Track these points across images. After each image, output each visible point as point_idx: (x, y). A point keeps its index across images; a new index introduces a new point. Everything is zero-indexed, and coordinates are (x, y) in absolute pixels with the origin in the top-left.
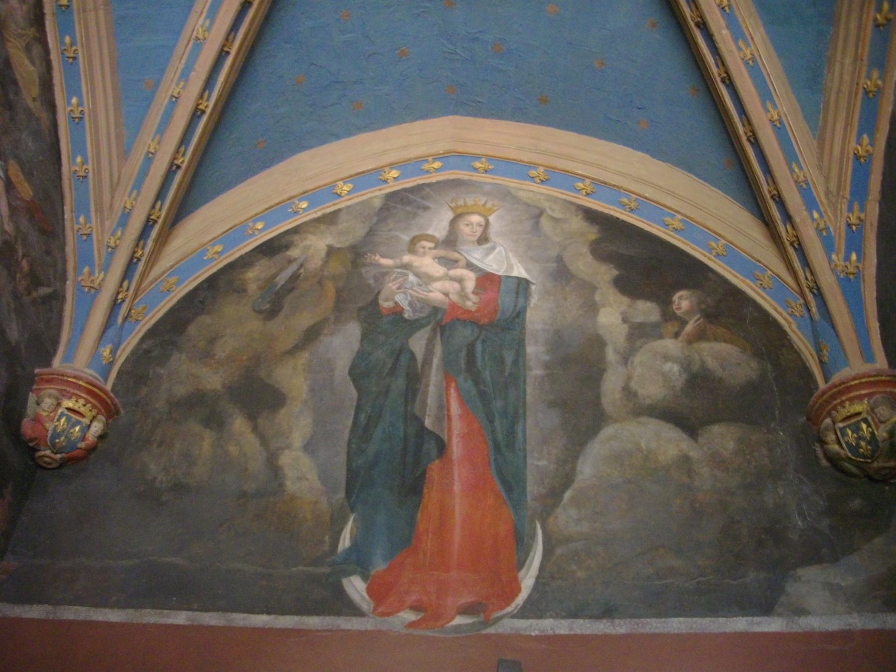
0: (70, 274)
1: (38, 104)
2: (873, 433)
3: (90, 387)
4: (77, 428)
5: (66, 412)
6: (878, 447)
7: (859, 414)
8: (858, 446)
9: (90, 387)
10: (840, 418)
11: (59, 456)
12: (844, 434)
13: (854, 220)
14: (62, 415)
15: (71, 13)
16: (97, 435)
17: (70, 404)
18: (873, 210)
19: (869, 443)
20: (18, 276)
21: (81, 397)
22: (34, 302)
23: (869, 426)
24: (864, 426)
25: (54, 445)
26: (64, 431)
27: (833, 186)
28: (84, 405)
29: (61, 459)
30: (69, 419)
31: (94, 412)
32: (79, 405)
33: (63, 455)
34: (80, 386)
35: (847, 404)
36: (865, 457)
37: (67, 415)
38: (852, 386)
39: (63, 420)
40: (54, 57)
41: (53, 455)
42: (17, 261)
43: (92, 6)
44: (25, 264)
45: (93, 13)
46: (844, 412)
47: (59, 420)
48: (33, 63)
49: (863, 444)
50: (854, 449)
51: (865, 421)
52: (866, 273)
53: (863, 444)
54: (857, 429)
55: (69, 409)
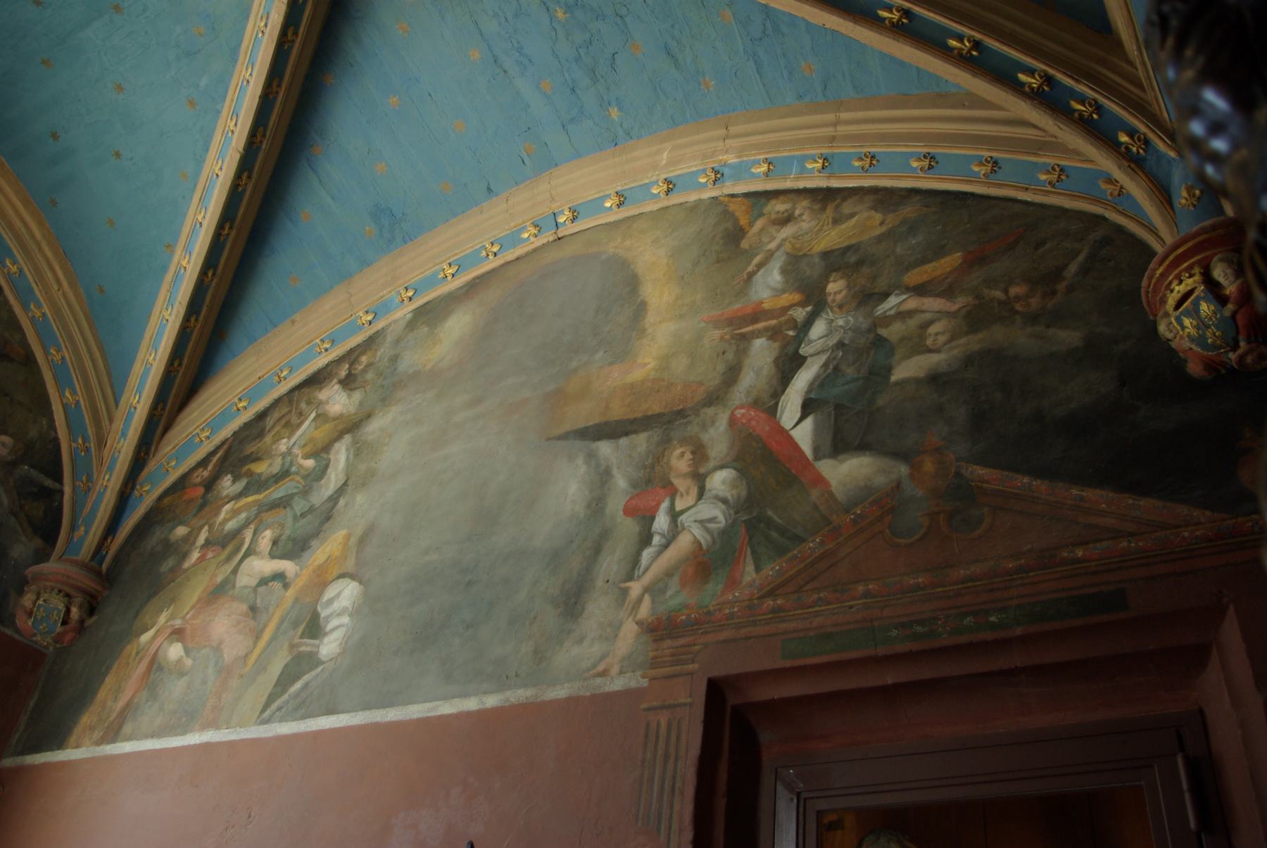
0: (1097, 210)
1: (891, 217)
3: (1167, 262)
4: (1204, 307)
5: (1178, 313)
9: (1167, 262)
11: (1242, 344)
14: (1179, 320)
15: (833, 155)
16: (1231, 278)
17: (1172, 300)
20: (1018, 307)
21: (1170, 283)
22: (1071, 289)
25: (1214, 347)
26: (1197, 327)
28: (1181, 282)
29: (1249, 342)
30: (1187, 314)
31: (1197, 270)
32: (1179, 289)
33: (1241, 338)
34: (1161, 275)
37: (1181, 313)
39: (1187, 322)
40: (867, 183)
41: (1240, 351)
42: (1001, 303)
43: (832, 129)
44: (1015, 290)
45: (839, 128)
47: (1183, 327)
48: (852, 215)
55: (1177, 307)
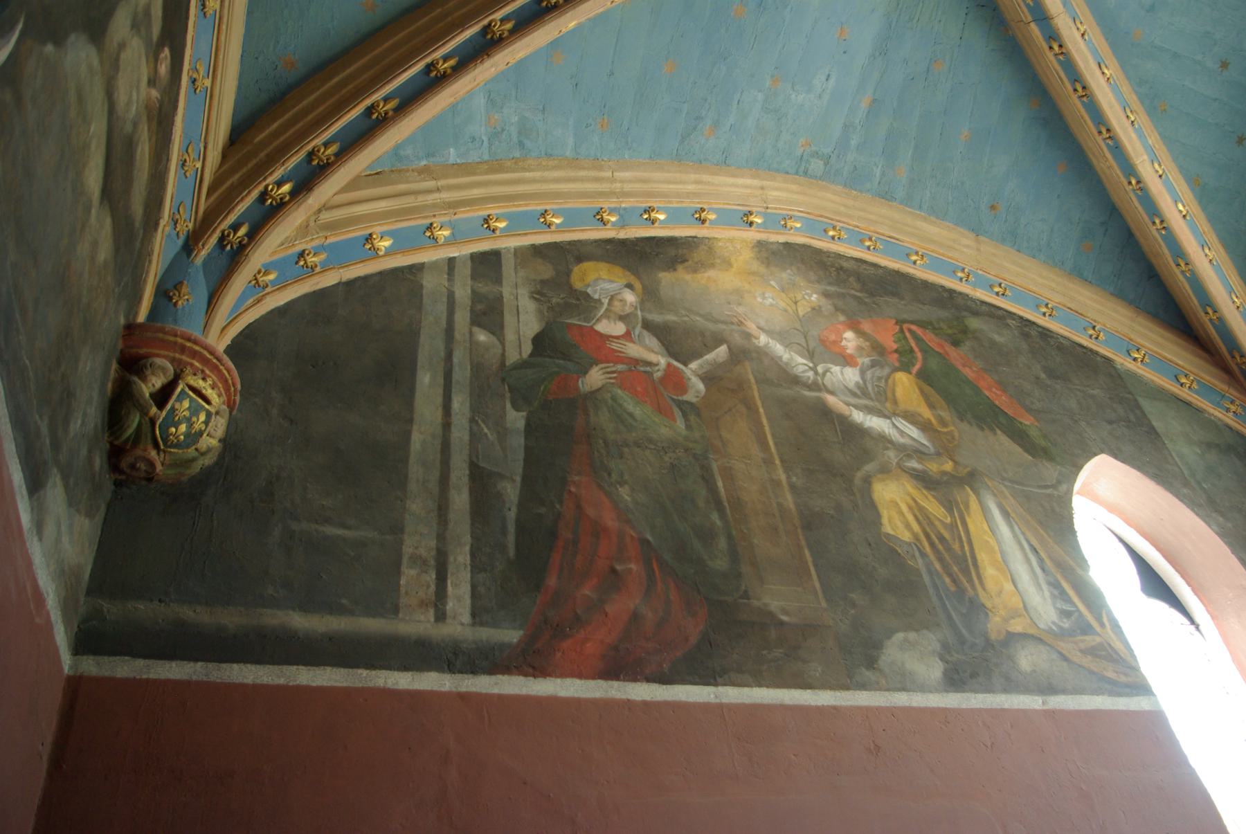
2: (200, 433)
6: (188, 447)
7: (208, 402)
8: (177, 426)
10: (192, 382)
12: (180, 399)
13: (311, 259)
18: (329, 280)
19: (187, 435)
23: (207, 423)
24: (202, 417)
27: (326, 217)
35: (210, 382)
36: (165, 441)
38: (220, 371)
46: (200, 384)
49: (183, 428)
50: (171, 420)
51: (209, 415)
52: (268, 299)
53: (183, 428)
54: (195, 411)
